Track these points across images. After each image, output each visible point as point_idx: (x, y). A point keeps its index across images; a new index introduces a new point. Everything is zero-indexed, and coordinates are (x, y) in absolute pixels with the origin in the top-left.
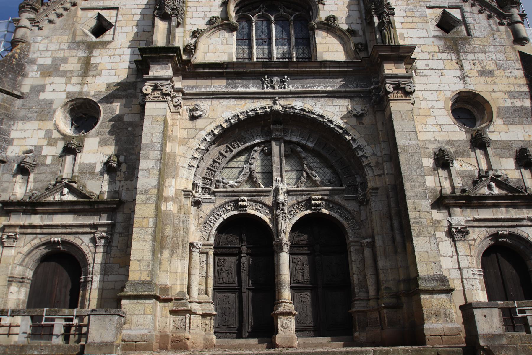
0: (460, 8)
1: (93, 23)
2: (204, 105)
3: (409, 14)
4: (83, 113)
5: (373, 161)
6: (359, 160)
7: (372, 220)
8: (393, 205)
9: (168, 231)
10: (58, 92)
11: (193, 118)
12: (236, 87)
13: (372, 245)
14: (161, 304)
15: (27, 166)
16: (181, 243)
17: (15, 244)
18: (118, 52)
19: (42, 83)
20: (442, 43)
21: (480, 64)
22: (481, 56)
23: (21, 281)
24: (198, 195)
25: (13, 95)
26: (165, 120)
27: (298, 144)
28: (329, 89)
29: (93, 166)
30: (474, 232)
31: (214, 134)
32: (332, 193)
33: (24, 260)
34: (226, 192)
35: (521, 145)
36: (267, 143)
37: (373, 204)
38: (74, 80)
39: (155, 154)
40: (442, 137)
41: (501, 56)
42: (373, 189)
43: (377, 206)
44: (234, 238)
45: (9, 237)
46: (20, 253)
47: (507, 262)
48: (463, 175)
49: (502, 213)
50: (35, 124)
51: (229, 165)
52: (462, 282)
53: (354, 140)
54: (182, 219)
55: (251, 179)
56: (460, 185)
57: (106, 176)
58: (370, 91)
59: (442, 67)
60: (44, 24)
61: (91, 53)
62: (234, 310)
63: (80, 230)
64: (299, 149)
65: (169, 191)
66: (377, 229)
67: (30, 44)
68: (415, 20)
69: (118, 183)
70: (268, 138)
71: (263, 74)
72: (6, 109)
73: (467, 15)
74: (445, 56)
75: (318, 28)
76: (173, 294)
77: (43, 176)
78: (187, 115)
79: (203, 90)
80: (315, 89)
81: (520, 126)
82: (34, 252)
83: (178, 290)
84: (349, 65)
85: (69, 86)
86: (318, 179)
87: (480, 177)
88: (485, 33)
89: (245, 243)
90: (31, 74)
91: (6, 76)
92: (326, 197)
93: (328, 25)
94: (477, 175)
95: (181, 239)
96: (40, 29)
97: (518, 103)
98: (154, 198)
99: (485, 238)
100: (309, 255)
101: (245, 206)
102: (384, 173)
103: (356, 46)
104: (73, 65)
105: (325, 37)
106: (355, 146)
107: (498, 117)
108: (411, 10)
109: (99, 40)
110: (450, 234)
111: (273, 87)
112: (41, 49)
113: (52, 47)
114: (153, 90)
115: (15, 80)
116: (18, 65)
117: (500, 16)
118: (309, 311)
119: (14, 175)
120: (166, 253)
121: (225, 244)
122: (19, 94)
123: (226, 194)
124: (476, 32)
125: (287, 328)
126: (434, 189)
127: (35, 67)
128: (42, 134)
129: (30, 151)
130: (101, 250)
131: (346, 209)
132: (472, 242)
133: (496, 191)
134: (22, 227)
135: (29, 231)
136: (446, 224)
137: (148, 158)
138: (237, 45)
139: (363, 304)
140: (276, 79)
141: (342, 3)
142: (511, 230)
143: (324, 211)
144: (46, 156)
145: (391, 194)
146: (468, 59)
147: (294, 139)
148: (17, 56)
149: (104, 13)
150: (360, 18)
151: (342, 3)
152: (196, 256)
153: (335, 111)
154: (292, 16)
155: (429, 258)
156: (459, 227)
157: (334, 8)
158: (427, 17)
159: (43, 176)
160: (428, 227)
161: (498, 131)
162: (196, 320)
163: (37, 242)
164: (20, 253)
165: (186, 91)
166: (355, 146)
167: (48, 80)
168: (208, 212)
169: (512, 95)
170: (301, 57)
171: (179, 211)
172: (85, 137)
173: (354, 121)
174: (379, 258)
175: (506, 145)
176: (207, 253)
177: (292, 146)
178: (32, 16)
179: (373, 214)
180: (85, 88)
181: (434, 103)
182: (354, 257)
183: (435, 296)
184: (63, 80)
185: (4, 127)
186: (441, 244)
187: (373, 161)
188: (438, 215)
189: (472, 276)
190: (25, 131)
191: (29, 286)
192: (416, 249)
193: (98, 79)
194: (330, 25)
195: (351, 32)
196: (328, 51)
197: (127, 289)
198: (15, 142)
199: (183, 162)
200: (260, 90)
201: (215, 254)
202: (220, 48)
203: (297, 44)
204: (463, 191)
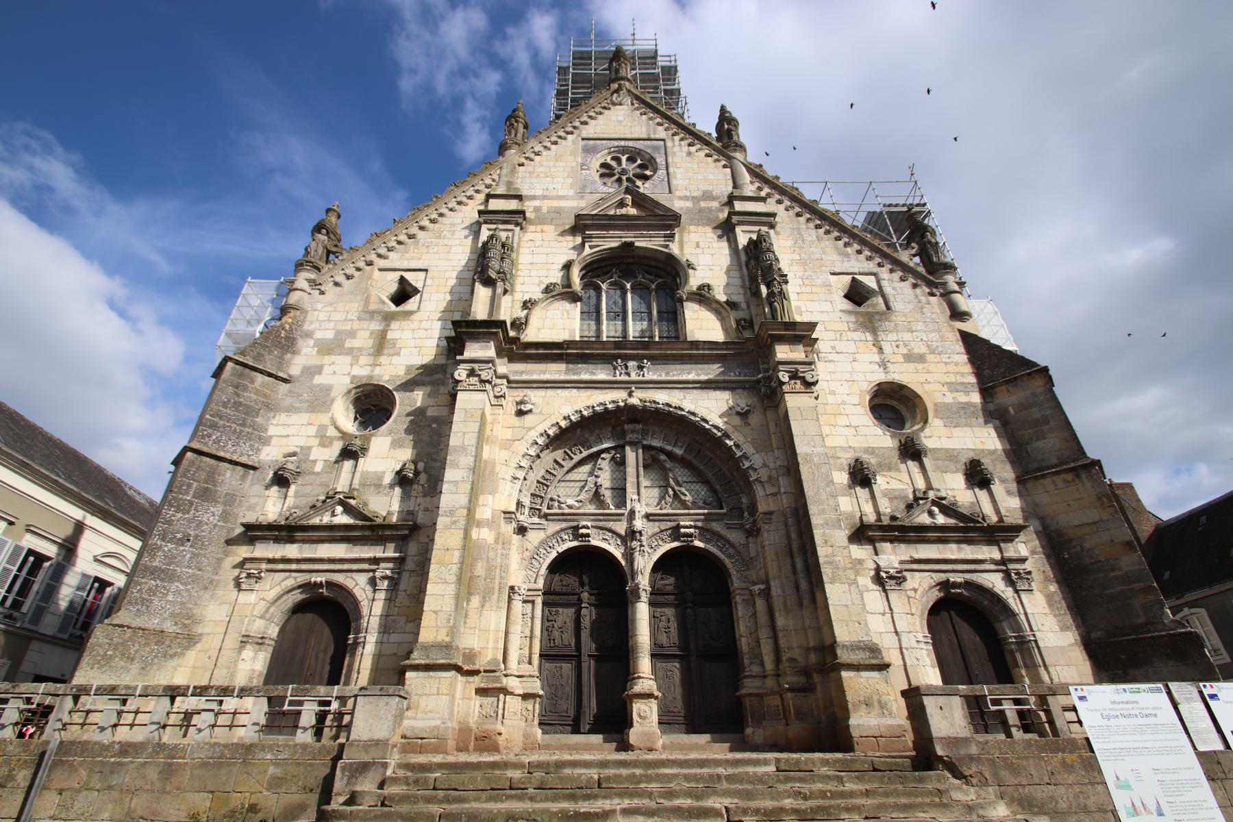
0: (874, 274)
1: (394, 288)
2: (536, 397)
3: (806, 282)
4: (373, 405)
5: (764, 474)
6: (745, 474)
7: (765, 558)
8: (794, 536)
9: (480, 569)
10: (341, 375)
11: (520, 413)
12: (580, 374)
13: (767, 594)
14: (464, 679)
15: (287, 475)
16: (497, 587)
17: (257, 587)
18: (425, 325)
19: (319, 363)
20: (853, 319)
21: (906, 346)
22: (907, 336)
23: (261, 642)
24: (524, 518)
25: (277, 378)
26: (483, 416)
27: (662, 450)
28: (703, 378)
29: (380, 477)
30: (913, 578)
31: (548, 436)
32: (708, 518)
33: (267, 611)
34: (563, 514)
35: (971, 455)
36: (620, 448)
37: (765, 535)
38: (364, 360)
39: (467, 461)
40: (859, 443)
41: (934, 336)
42: (765, 514)
43: (772, 537)
44: (571, 581)
45: (249, 576)
46: (263, 599)
47: (965, 625)
48: (892, 496)
49: (952, 551)
50: (304, 417)
51: (568, 477)
52: (902, 653)
53: (737, 446)
54: (500, 552)
55: (597, 497)
56: (889, 510)
57: (398, 490)
58: (758, 381)
59: (854, 350)
60: (328, 287)
61: (388, 325)
62: (570, 689)
63: (355, 567)
64: (663, 457)
65: (484, 513)
66: (773, 571)
67: (306, 312)
68: (815, 289)
69: (413, 499)
70: (621, 442)
71: (616, 357)
72: (265, 396)
73: (884, 283)
74: (858, 335)
75: (687, 300)
76: (480, 664)
77: (308, 489)
78: (513, 409)
79: (535, 377)
80: (684, 377)
81: (967, 429)
82: (285, 598)
83: (489, 658)
85: (355, 367)
86: (689, 498)
87: (916, 499)
88: (910, 306)
89: (587, 588)
90: (305, 351)
91: (270, 352)
92: (700, 524)
93: (700, 295)
94: (911, 497)
95: (497, 581)
96: (322, 293)
97: (963, 398)
98: (462, 522)
99: (931, 588)
100: (676, 606)
101: (588, 535)
102: (779, 492)
103: (738, 322)
104: (363, 340)
106: (739, 454)
107: (936, 416)
109: (400, 309)
110: (878, 580)
111: (629, 375)
112: (321, 318)
113: (337, 316)
114: (468, 376)
115: (281, 358)
116: (287, 338)
117: (930, 284)
118: (678, 692)
119: (267, 487)
120: (475, 601)
121: (558, 589)
122: (285, 376)
123: (562, 517)
124: (897, 305)
125: (646, 717)
126: (850, 516)
127: (311, 342)
128: (312, 430)
129: (294, 454)
130: (381, 595)
131: (727, 541)
132: (911, 594)
133: (941, 519)
134: (270, 561)
135: (281, 566)
136: (873, 566)
137: (457, 466)
138: (582, 319)
139: (758, 682)
140: (632, 364)
142: (968, 576)
143: (698, 543)
144: (315, 461)
145: (791, 521)
146: (889, 340)
147: (656, 443)
148: (287, 327)
149: (408, 276)
150: (743, 286)
152: (517, 605)
153: (712, 409)
155: (850, 615)
156: (892, 571)
157: (709, 274)
159: (308, 489)
160: (845, 569)
161: (934, 436)
162: (514, 704)
163: (290, 583)
164: (263, 599)
165: (512, 378)
166: (739, 454)
167: (327, 359)
168: (536, 542)
169: (953, 387)
171: (496, 541)
172: (372, 435)
173: (737, 420)
174: (777, 614)
175: (950, 456)
176: (533, 602)
177: (653, 452)
178: (312, 276)
179: (767, 548)
180: (377, 371)
181: (846, 398)
182: (741, 611)
183: (864, 674)
184: (348, 359)
185: (259, 420)
186: (866, 595)
187: (764, 474)
188: (860, 552)
189: (915, 645)
190: (289, 425)
191: (271, 649)
192: (830, 602)
193: (395, 360)
194: (703, 296)
195: (732, 305)
197: (415, 654)
198: (274, 441)
199: (505, 473)
200: (611, 378)
201: (544, 604)
202: (559, 323)
203: (660, 319)
204: (893, 518)
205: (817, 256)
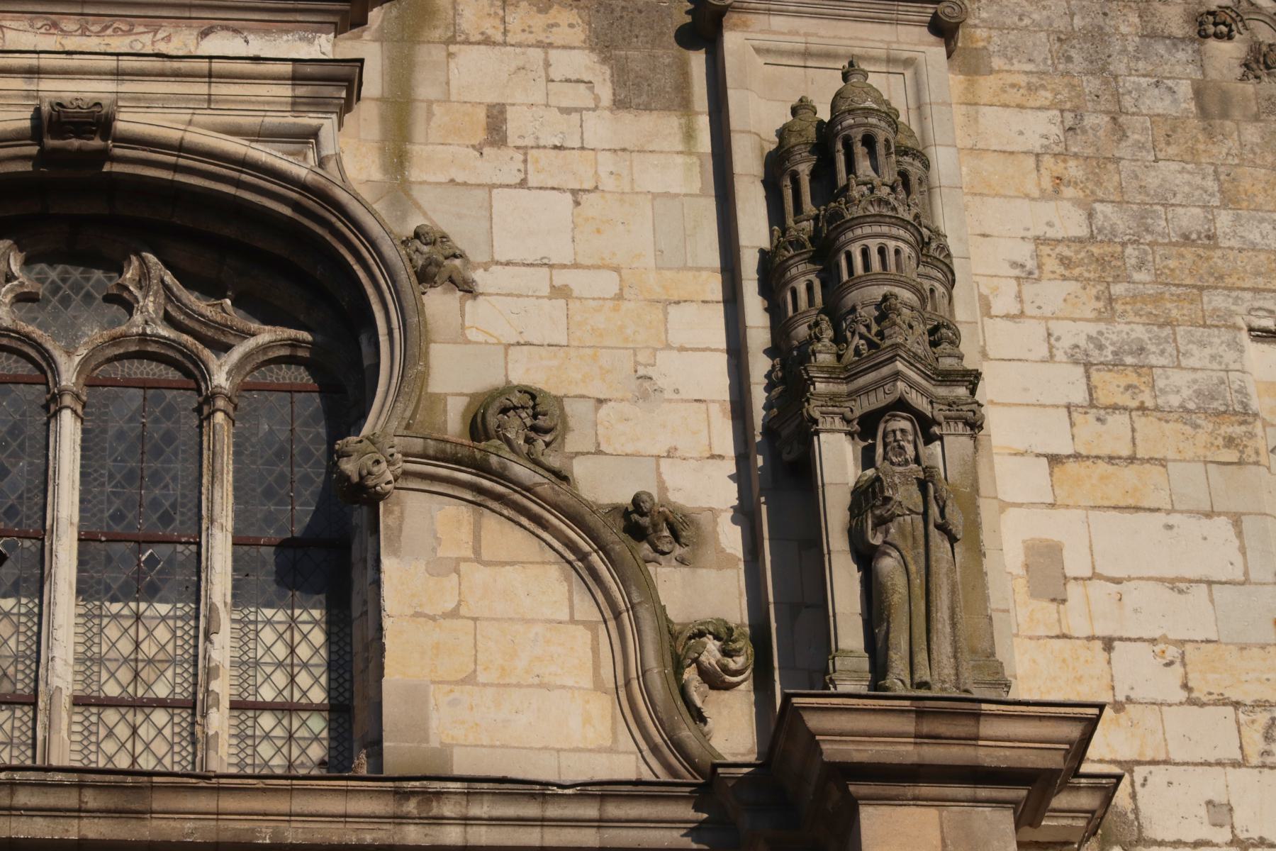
68: (1157, 436)
84: (613, 810)
105: (455, 567)
108: (1131, 359)
141: (607, 283)
151: (607, 283)
154: (222, 348)
157: (545, 321)
158: (1246, 415)
170: (267, 694)
196: (470, 680)
205: (1189, 218)
